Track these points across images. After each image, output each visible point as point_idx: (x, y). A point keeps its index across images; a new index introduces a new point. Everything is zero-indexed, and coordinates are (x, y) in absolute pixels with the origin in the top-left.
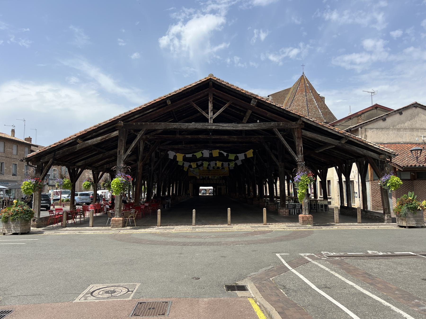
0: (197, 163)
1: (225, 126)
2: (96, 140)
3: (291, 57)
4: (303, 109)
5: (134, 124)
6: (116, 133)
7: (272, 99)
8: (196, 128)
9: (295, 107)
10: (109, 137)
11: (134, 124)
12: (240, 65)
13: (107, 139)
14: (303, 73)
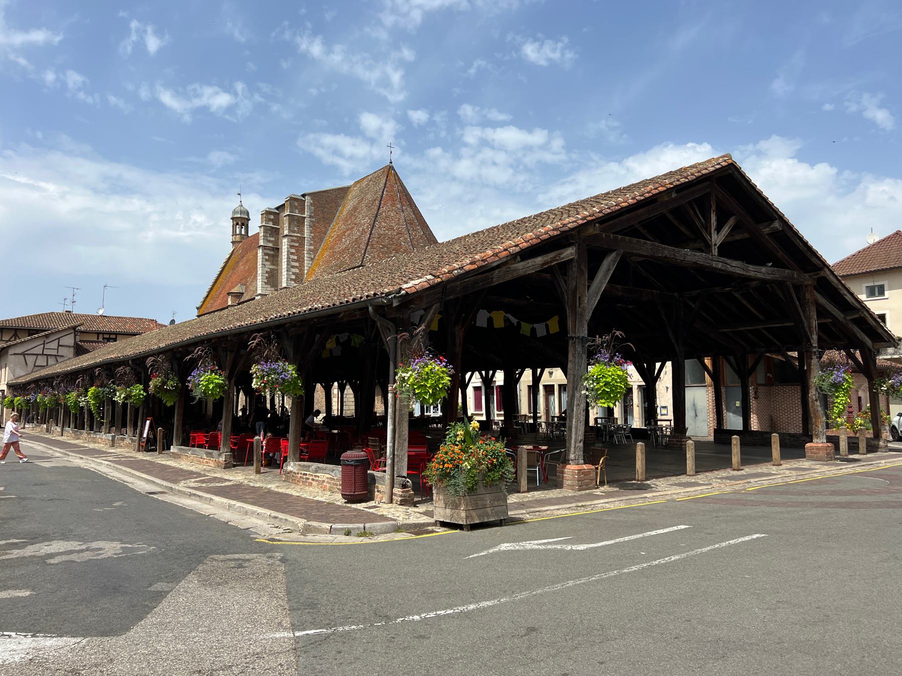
0: (337, 337)
1: (734, 265)
2: (533, 263)
3: (213, 109)
5: (604, 235)
6: (569, 253)
7: (311, 204)
8: (695, 263)
9: (384, 230)
10: (558, 260)
11: (604, 235)
12: (81, 95)
13: (552, 264)
14: (391, 163)
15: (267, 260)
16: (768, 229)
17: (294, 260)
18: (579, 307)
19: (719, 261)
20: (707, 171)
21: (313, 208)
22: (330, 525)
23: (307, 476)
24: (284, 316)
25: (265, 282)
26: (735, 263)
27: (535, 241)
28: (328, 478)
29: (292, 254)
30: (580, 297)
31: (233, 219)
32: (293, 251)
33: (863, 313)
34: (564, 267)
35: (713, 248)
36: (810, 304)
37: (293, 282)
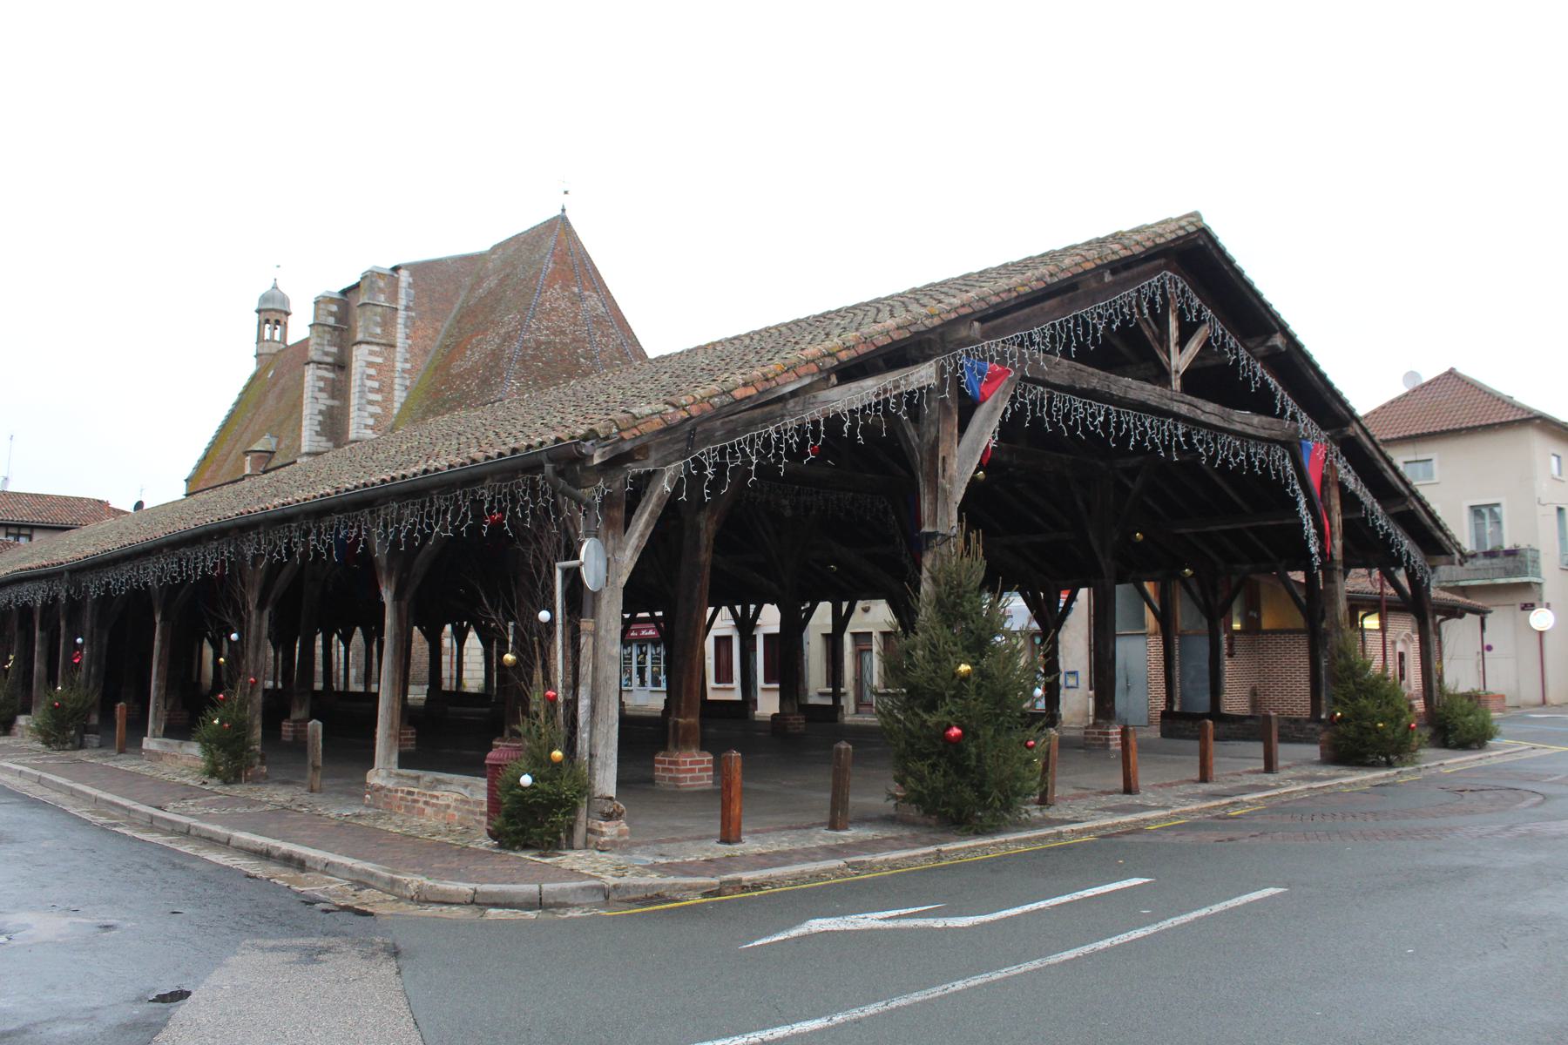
1: (1208, 410)
4: (579, 348)
6: (924, 375)
7: (409, 284)
9: (547, 335)
14: (563, 210)
15: (321, 390)
16: (1262, 349)
17: (372, 390)
18: (943, 476)
19: (1183, 402)
20: (1163, 240)
21: (412, 292)
22: (473, 886)
23: (415, 797)
24: (373, 484)
25: (316, 432)
26: (1210, 407)
27: (862, 349)
28: (456, 800)
29: (370, 377)
30: (944, 458)
31: (259, 311)
32: (372, 372)
33: (1412, 503)
34: (913, 402)
35: (1173, 377)
36: (1330, 485)
37: (370, 432)
